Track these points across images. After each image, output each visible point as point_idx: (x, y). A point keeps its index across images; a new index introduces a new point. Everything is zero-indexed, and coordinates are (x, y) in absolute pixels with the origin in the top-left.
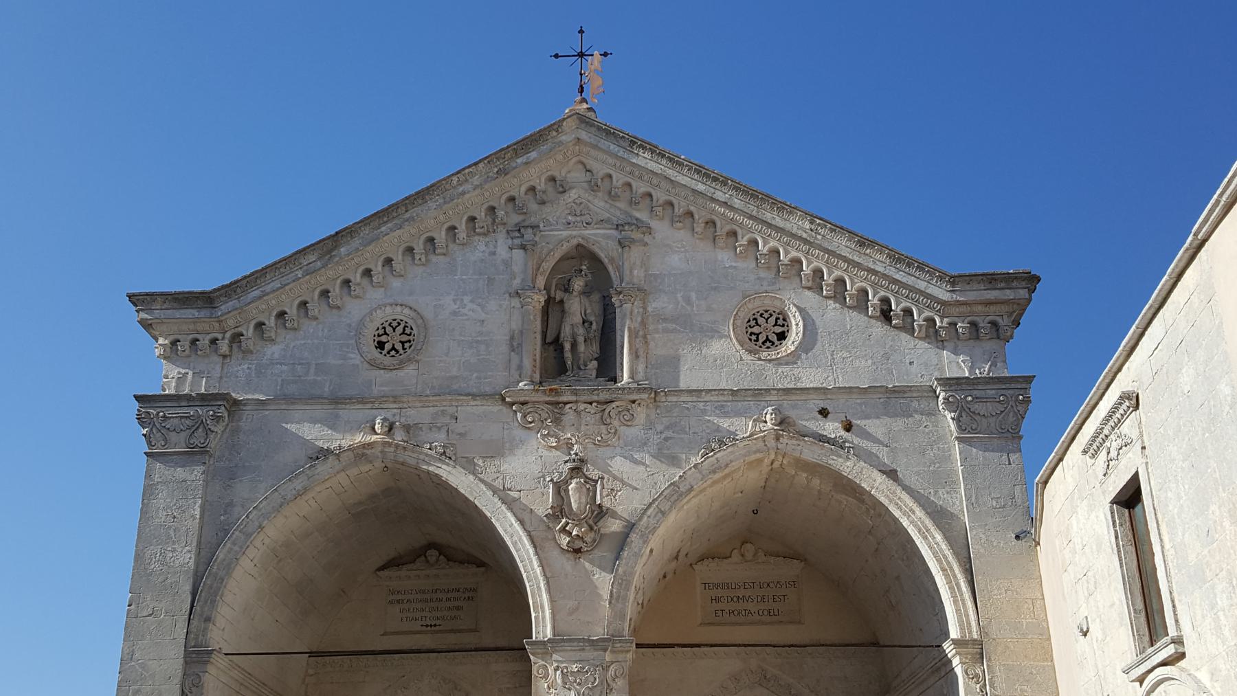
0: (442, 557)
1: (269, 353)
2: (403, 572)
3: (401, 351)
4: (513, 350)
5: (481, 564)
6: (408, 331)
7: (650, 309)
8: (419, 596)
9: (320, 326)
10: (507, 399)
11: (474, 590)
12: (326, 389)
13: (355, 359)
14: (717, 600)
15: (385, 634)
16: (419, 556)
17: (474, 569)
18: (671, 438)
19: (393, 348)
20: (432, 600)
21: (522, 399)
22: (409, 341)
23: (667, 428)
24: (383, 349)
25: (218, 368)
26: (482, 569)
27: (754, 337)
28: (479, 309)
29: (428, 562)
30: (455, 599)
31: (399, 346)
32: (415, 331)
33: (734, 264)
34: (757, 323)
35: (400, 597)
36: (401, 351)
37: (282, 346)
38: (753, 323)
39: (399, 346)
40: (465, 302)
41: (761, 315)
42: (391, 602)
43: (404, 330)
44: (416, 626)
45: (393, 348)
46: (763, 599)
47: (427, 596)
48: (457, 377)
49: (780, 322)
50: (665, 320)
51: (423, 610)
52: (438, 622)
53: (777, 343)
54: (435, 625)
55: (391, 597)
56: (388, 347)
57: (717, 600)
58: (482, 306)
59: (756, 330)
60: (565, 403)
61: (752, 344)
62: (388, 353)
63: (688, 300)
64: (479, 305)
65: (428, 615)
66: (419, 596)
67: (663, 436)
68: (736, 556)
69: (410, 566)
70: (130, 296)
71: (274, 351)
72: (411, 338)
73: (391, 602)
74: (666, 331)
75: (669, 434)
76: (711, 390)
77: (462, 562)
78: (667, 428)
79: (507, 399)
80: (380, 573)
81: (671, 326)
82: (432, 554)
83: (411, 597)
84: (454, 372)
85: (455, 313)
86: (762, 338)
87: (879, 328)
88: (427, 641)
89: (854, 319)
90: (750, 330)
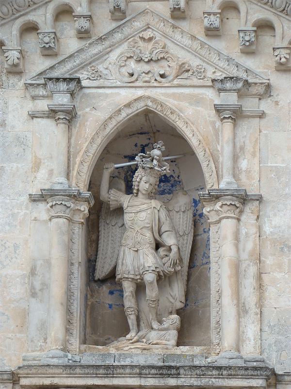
4: (34, 295)
7: (267, 229)
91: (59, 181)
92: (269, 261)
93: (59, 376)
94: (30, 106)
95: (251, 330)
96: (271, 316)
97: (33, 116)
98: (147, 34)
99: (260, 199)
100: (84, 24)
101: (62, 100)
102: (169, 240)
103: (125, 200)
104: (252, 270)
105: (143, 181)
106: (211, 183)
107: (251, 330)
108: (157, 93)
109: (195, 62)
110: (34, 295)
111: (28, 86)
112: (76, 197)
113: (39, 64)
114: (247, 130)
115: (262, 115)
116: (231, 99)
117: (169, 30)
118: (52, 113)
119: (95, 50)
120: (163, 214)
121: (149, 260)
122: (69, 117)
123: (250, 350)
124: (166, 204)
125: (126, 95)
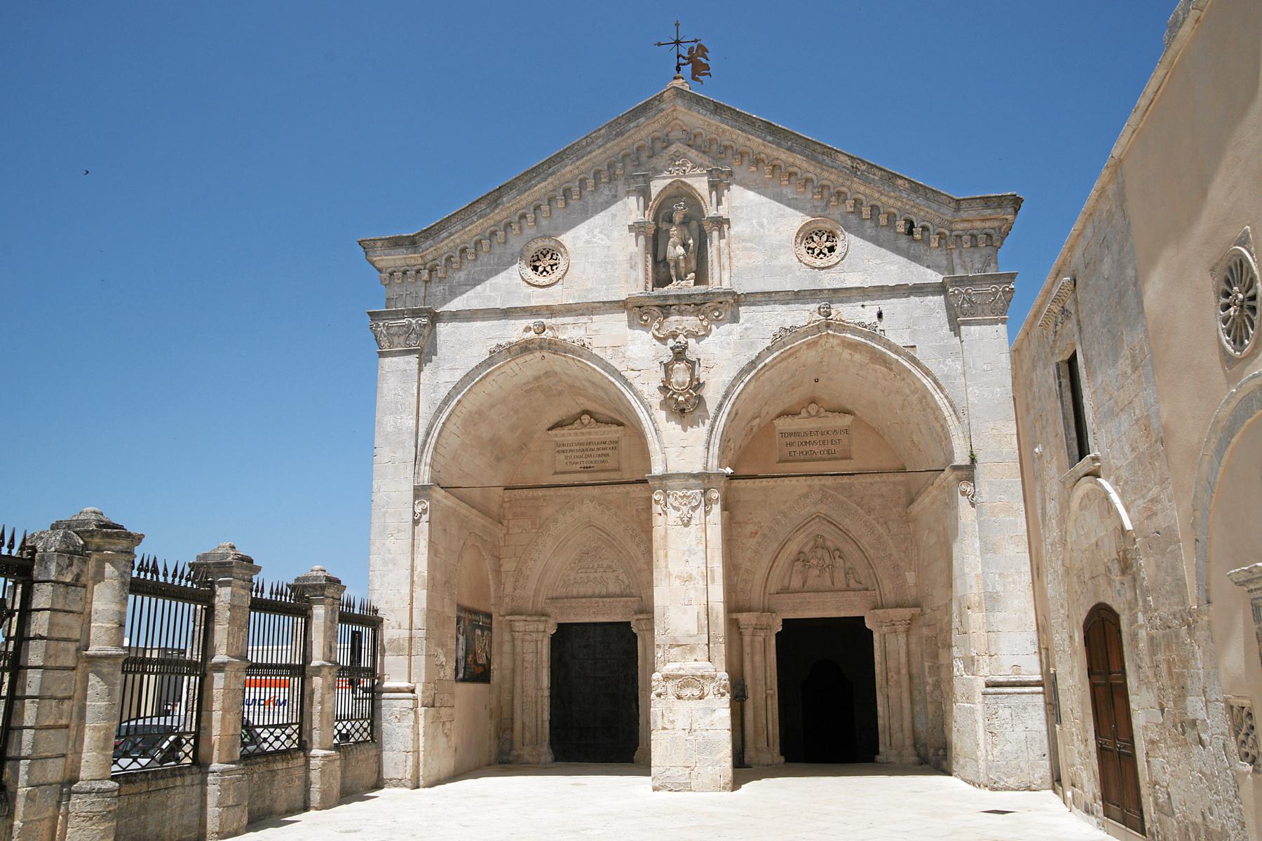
0: (592, 420)
1: (457, 277)
2: (565, 431)
3: (551, 272)
4: (631, 268)
5: (620, 424)
8: (578, 447)
9: (492, 256)
11: (617, 442)
14: (791, 444)
15: (556, 473)
17: (614, 428)
18: (750, 328)
20: (587, 450)
22: (556, 264)
24: (537, 271)
25: (423, 289)
26: (621, 428)
27: (810, 251)
28: (605, 238)
29: (583, 423)
30: (604, 449)
31: (548, 269)
33: (795, 196)
34: (813, 241)
35: (565, 448)
36: (551, 272)
37: (466, 272)
39: (548, 269)
40: (595, 233)
41: (816, 234)
42: (558, 452)
43: (552, 256)
44: (577, 467)
46: (824, 443)
47: (584, 447)
48: (591, 289)
50: (743, 241)
51: (581, 457)
52: (592, 465)
53: (828, 254)
55: (558, 449)
56: (540, 269)
57: (791, 444)
58: (608, 237)
62: (541, 273)
63: (761, 225)
64: (606, 235)
65: (584, 460)
66: (578, 447)
68: (804, 412)
69: (570, 427)
73: (558, 452)
74: (745, 249)
75: (748, 325)
77: (607, 423)
80: (550, 432)
81: (749, 245)
82: (586, 418)
83: (572, 448)
84: (589, 285)
85: (588, 242)
88: (584, 478)
90: (808, 246)
95: (726, 276)
96: (735, 270)
104: (727, 251)
107: (726, 276)
110: (631, 268)
123: (726, 285)
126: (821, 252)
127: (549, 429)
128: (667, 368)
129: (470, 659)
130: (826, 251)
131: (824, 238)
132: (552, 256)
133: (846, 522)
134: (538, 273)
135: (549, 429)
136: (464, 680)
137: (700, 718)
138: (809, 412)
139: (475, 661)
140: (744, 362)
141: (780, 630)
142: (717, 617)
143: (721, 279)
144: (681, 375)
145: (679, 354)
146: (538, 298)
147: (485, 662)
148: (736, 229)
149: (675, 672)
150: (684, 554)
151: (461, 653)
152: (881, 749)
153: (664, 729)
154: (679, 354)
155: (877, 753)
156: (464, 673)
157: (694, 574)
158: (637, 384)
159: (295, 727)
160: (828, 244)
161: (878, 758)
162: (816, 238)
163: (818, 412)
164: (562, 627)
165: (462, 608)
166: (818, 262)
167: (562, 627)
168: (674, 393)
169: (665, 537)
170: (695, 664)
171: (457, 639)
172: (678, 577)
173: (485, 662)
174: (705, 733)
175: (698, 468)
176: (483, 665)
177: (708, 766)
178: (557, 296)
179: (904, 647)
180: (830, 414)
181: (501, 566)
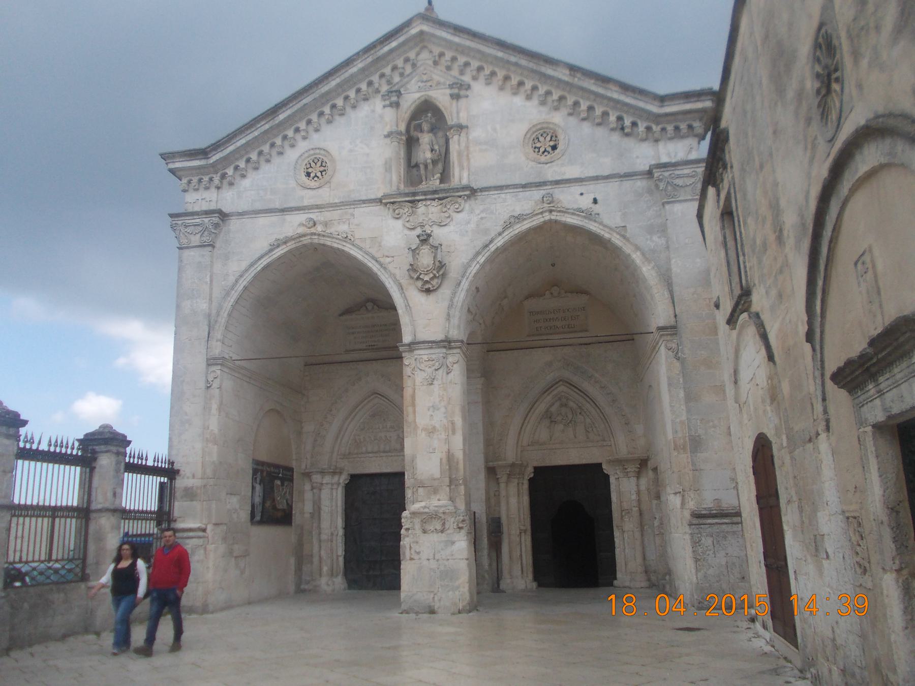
0: (375, 306)
3: (320, 177)
6: (324, 164)
7: (470, 138)
10: (383, 201)
12: (277, 203)
13: (293, 184)
16: (361, 307)
19: (316, 176)
21: (392, 200)
23: (482, 212)
25: (215, 195)
27: (537, 150)
31: (319, 174)
32: (328, 164)
34: (539, 141)
36: (320, 177)
38: (536, 141)
39: (319, 174)
41: (542, 135)
43: (322, 164)
45: (316, 176)
46: (564, 319)
49: (553, 139)
52: (375, 344)
53: (551, 152)
54: (374, 345)
56: (312, 175)
59: (538, 145)
60: (419, 201)
61: (535, 155)
63: (495, 130)
67: (480, 217)
70: (161, 155)
71: (246, 183)
72: (326, 168)
75: (483, 215)
76: (509, 186)
78: (482, 212)
79: (383, 201)
80: (341, 317)
82: (370, 305)
85: (351, 151)
86: (542, 150)
87: (616, 137)
88: (368, 355)
89: (601, 132)
91: (394, 128)
92: (471, 149)
93: (396, 198)
94: (383, 103)
95: (465, 175)
97: (384, 107)
98: (425, 72)
99: (467, 127)
100: (401, 70)
101: (394, 99)
102: (436, 147)
103: (420, 135)
104: (465, 153)
105: (426, 127)
106: (450, 123)
107: (465, 175)
108: (427, 93)
109: (442, 80)
111: (383, 96)
112: (400, 133)
113: (385, 88)
114: (463, 102)
115: (467, 96)
116: (456, 91)
117: (432, 69)
118: (391, 105)
119: (406, 80)
120: (433, 138)
121: (428, 155)
122: (397, 105)
123: (465, 182)
124: (435, 134)
125: (417, 95)
126: (545, 151)
127: (340, 315)
128: (414, 252)
129: (268, 504)
130: (549, 149)
131: (548, 138)
132: (322, 164)
133: (586, 386)
134: (311, 178)
135: (340, 315)
136: (262, 522)
137: (442, 549)
138: (552, 294)
139: (274, 508)
140: (479, 244)
141: (532, 475)
142: (458, 463)
143: (460, 176)
144: (426, 259)
145: (425, 239)
146: (308, 198)
147: (285, 507)
148: (477, 133)
149: (422, 510)
150: (429, 410)
151: (258, 500)
152: (619, 575)
153: (411, 559)
154: (425, 239)
155: (615, 578)
156: (262, 516)
157: (437, 426)
158: (391, 267)
159: (78, 562)
160: (552, 143)
161: (615, 582)
162: (541, 139)
163: (559, 293)
164: (354, 478)
165: (257, 463)
166: (543, 159)
167: (354, 478)
168: (421, 274)
169: (413, 397)
170: (439, 502)
171: (253, 488)
172: (424, 429)
173: (285, 507)
174: (447, 563)
175: (440, 337)
176: (284, 510)
177: (449, 591)
178: (325, 195)
179: (635, 488)
180: (569, 294)
181: (302, 428)
